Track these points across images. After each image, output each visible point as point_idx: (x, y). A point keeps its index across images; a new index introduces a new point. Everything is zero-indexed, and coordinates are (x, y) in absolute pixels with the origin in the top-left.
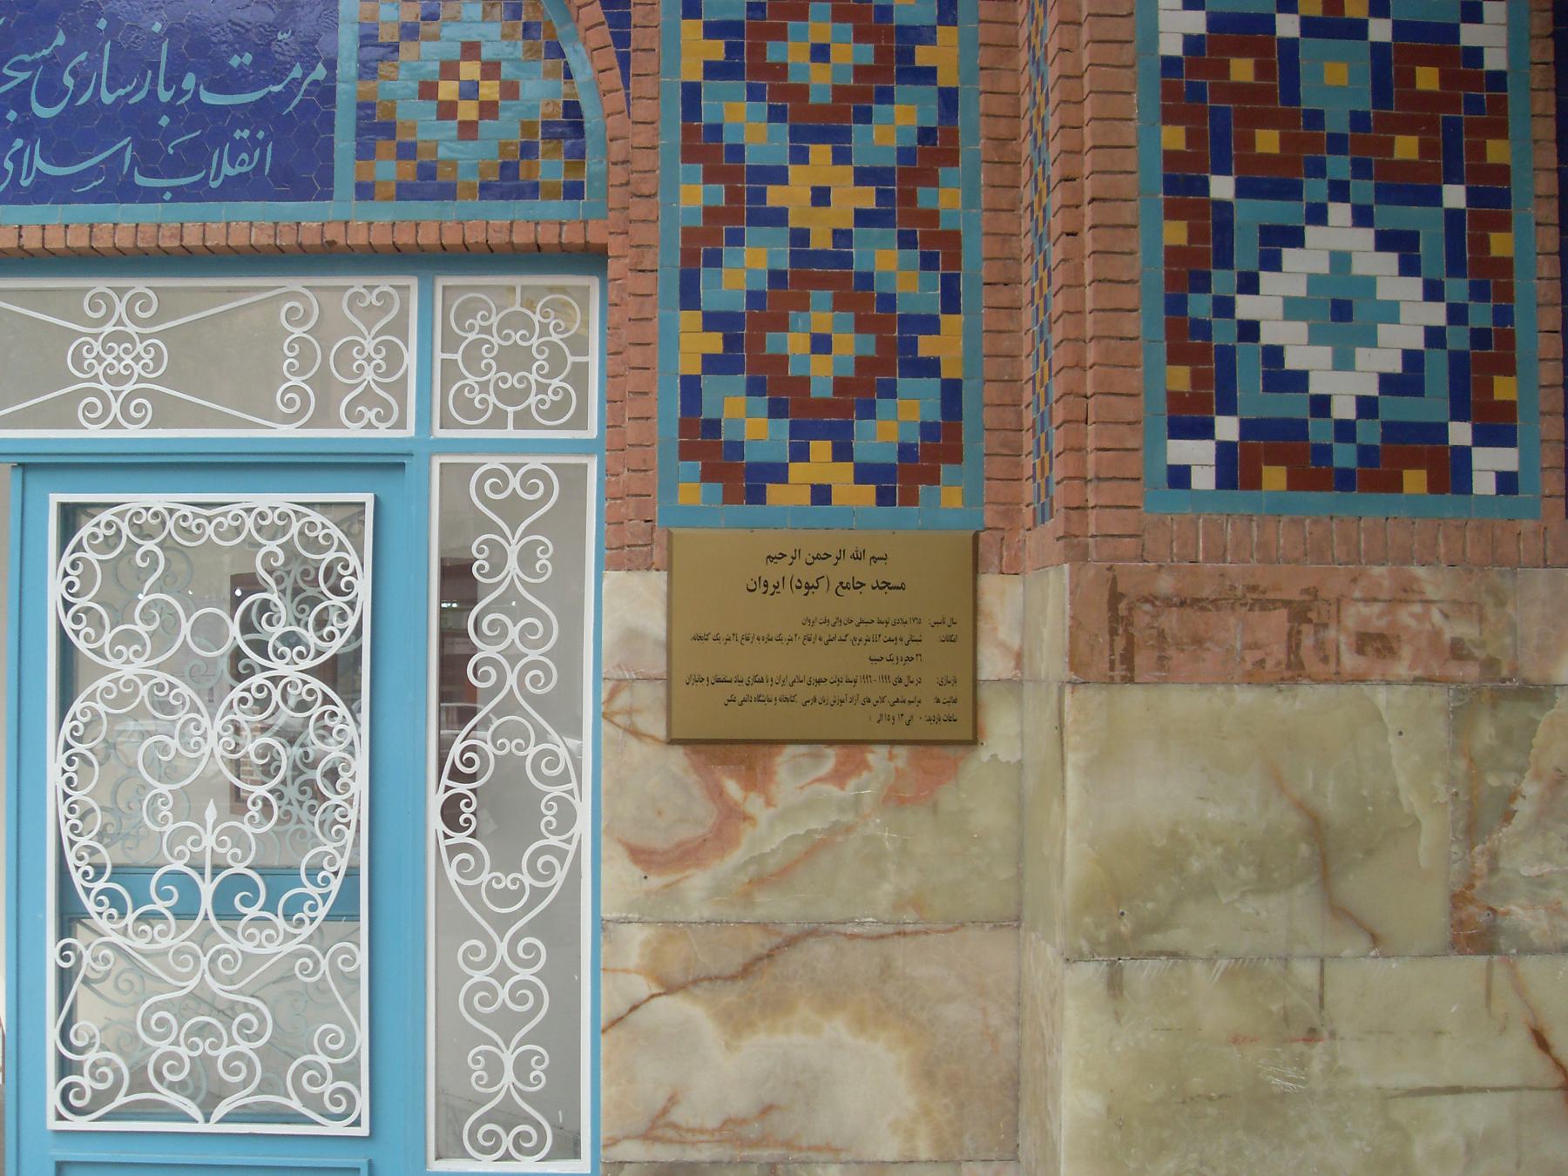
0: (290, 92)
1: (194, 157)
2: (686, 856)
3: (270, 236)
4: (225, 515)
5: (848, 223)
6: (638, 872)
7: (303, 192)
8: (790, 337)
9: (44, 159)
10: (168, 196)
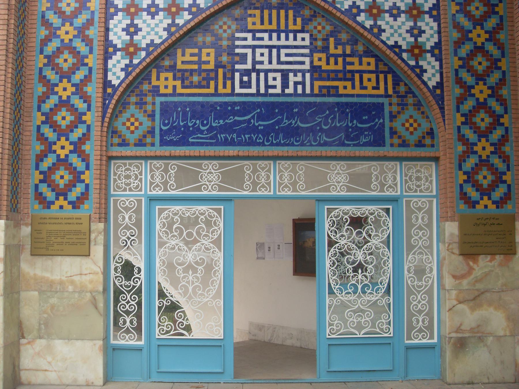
0: (375, 125)
1: (357, 138)
2: (463, 277)
4: (362, 210)
6: (454, 280)
7: (379, 145)
8: (479, 176)
9: (326, 137)
10: (352, 145)
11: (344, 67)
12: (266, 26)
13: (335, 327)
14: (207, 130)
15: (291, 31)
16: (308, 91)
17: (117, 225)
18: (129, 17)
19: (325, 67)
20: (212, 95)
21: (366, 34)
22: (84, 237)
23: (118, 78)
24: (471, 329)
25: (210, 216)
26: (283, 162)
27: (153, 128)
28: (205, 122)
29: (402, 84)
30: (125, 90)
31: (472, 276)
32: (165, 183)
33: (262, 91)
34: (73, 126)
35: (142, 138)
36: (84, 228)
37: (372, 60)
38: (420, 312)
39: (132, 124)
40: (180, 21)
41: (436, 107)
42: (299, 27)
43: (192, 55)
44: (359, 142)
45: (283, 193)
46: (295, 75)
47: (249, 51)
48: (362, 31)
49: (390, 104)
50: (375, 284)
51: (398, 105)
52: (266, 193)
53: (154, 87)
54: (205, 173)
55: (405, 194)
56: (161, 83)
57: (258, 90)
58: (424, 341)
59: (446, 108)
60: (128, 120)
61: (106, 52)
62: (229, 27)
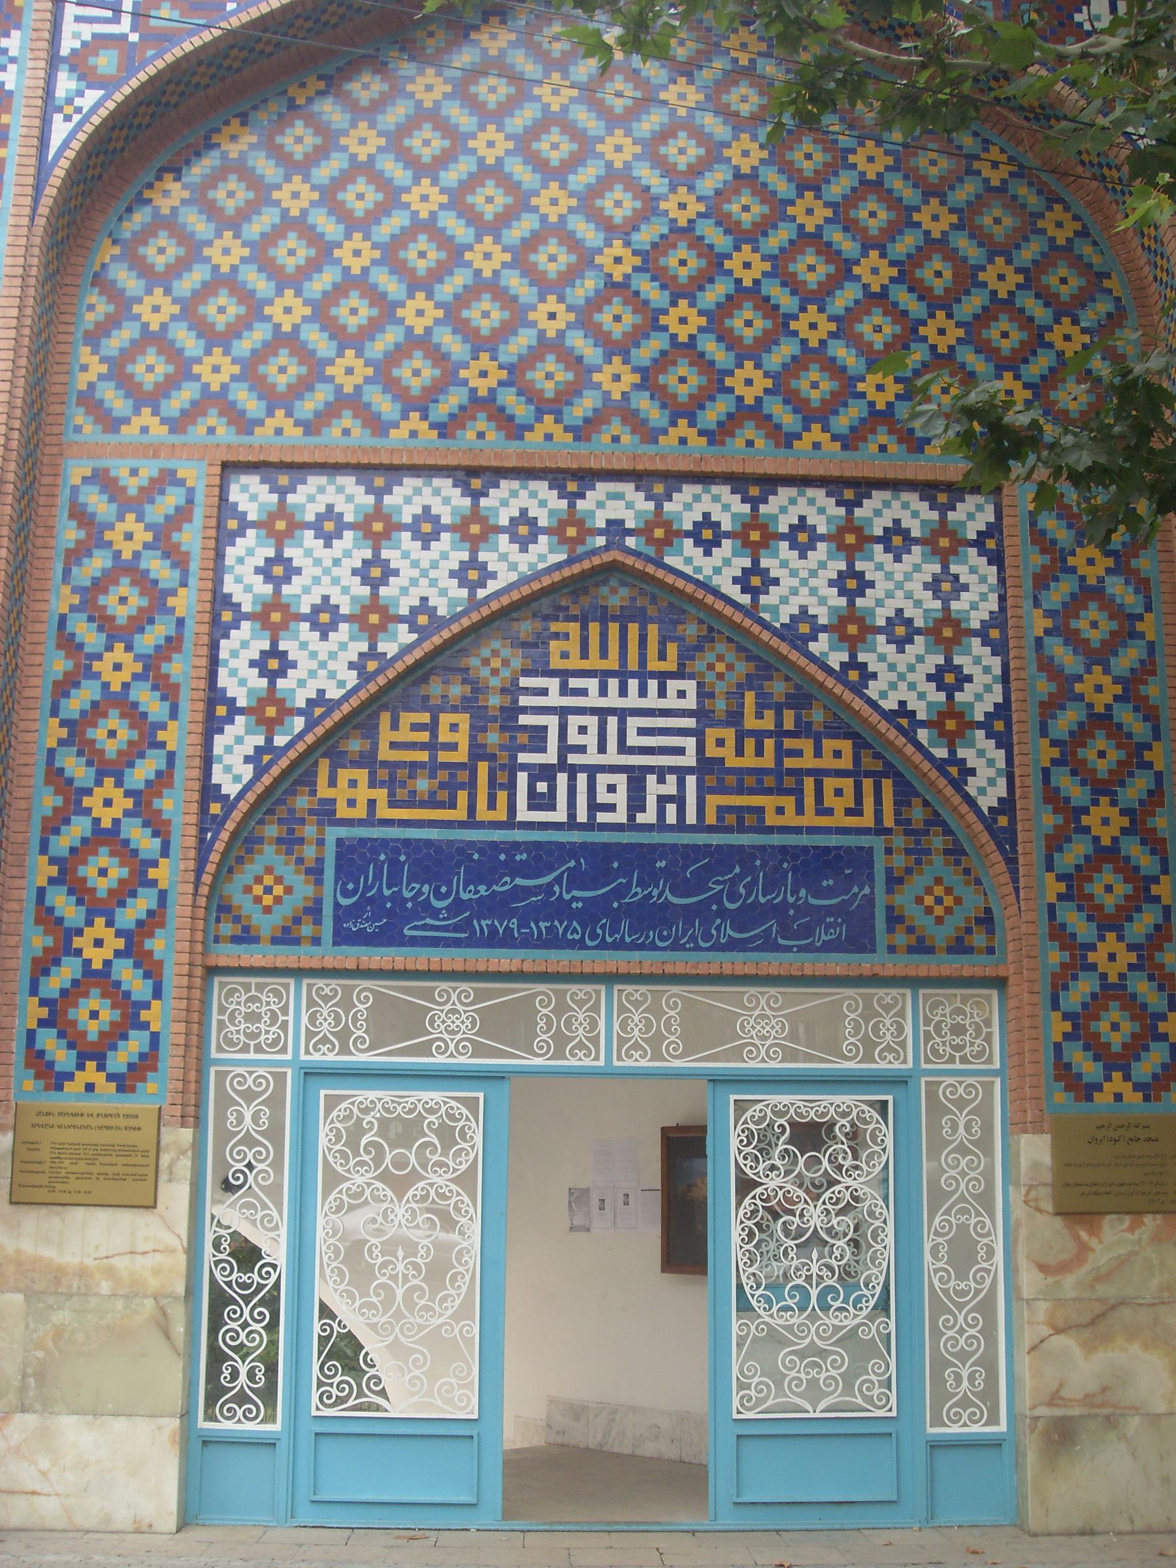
1: (807, 931)
2: (1064, 1268)
5: (1125, 970)
7: (861, 949)
11: (779, 762)
12: (594, 662)
13: (753, 1393)
14: (447, 908)
15: (653, 675)
16: (691, 818)
17: (223, 1135)
18: (267, 633)
19: (732, 762)
20: (461, 825)
21: (830, 683)
22: (144, 1161)
23: (237, 779)
24: (1087, 1396)
25: (452, 1117)
26: (629, 988)
27: (318, 901)
28: (444, 889)
30: (254, 807)
31: (1086, 1268)
32: (344, 1036)
33: (582, 816)
34: (123, 893)
36: (144, 1139)
37: (846, 746)
38: (963, 1356)
39: (268, 890)
40: (389, 648)
41: (997, 857)
42: (671, 665)
43: (415, 727)
45: (628, 1063)
46: (661, 780)
47: (552, 722)
48: (820, 676)
49: (889, 851)
50: (850, 1288)
51: (908, 852)
52: (588, 1062)
54: (439, 1012)
55: (924, 1066)
56: (341, 794)
57: (572, 815)
58: (975, 1429)
59: (1021, 860)
60: (259, 880)
61: (210, 714)
62: (506, 663)
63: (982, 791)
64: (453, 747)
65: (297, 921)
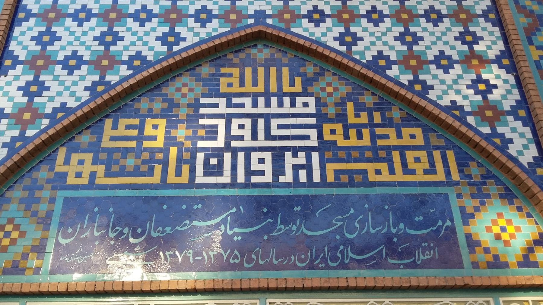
0: (438, 231)
3: (444, 282)
9: (353, 253)
10: (402, 267)
12: (249, 88)
15: (286, 95)
16: (317, 178)
19: (342, 143)
28: (139, 230)
29: (472, 164)
33: (241, 178)
35: (19, 259)
37: (418, 132)
42: (298, 89)
43: (128, 127)
44: (415, 260)
46: (295, 155)
47: (221, 123)
48: (396, 88)
49: (459, 196)
51: (473, 197)
53: (57, 174)
56: (72, 169)
62: (191, 90)
63: (520, 153)
64: (154, 138)
65: (25, 256)
